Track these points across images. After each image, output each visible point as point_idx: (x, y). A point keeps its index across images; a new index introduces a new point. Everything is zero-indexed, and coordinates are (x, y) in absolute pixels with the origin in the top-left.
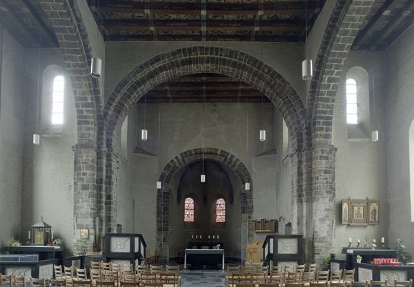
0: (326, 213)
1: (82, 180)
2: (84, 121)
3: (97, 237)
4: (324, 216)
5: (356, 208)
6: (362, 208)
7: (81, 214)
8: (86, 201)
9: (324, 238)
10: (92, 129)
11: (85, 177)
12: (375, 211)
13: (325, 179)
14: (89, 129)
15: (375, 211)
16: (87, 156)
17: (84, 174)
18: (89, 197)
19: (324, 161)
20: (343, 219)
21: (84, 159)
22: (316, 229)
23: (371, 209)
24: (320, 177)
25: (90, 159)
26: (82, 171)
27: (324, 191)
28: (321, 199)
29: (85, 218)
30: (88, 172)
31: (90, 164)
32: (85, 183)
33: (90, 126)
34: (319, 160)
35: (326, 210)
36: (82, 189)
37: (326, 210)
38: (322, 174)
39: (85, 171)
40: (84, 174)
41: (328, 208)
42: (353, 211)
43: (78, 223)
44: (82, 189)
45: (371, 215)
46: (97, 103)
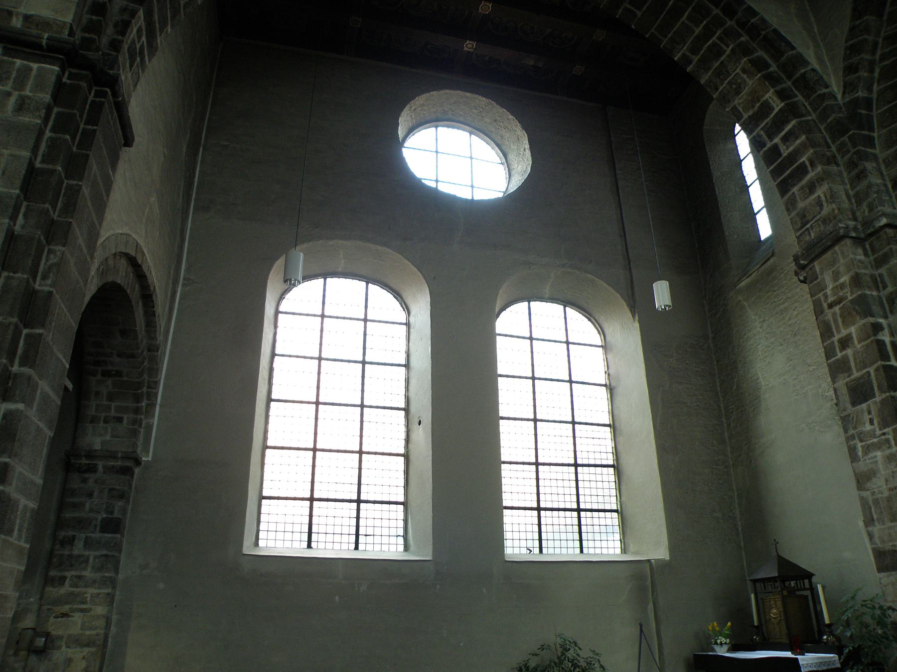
2: (790, 176)
8: (878, 446)
10: (820, 180)
11: (849, 352)
14: (811, 187)
16: (836, 276)
17: (845, 343)
18: (884, 424)
21: (829, 291)
25: (845, 279)
30: (853, 329)
31: (850, 298)
32: (856, 374)
33: (811, 175)
36: (854, 404)
39: (844, 333)
40: (845, 343)
44: (854, 404)
46: (807, 97)
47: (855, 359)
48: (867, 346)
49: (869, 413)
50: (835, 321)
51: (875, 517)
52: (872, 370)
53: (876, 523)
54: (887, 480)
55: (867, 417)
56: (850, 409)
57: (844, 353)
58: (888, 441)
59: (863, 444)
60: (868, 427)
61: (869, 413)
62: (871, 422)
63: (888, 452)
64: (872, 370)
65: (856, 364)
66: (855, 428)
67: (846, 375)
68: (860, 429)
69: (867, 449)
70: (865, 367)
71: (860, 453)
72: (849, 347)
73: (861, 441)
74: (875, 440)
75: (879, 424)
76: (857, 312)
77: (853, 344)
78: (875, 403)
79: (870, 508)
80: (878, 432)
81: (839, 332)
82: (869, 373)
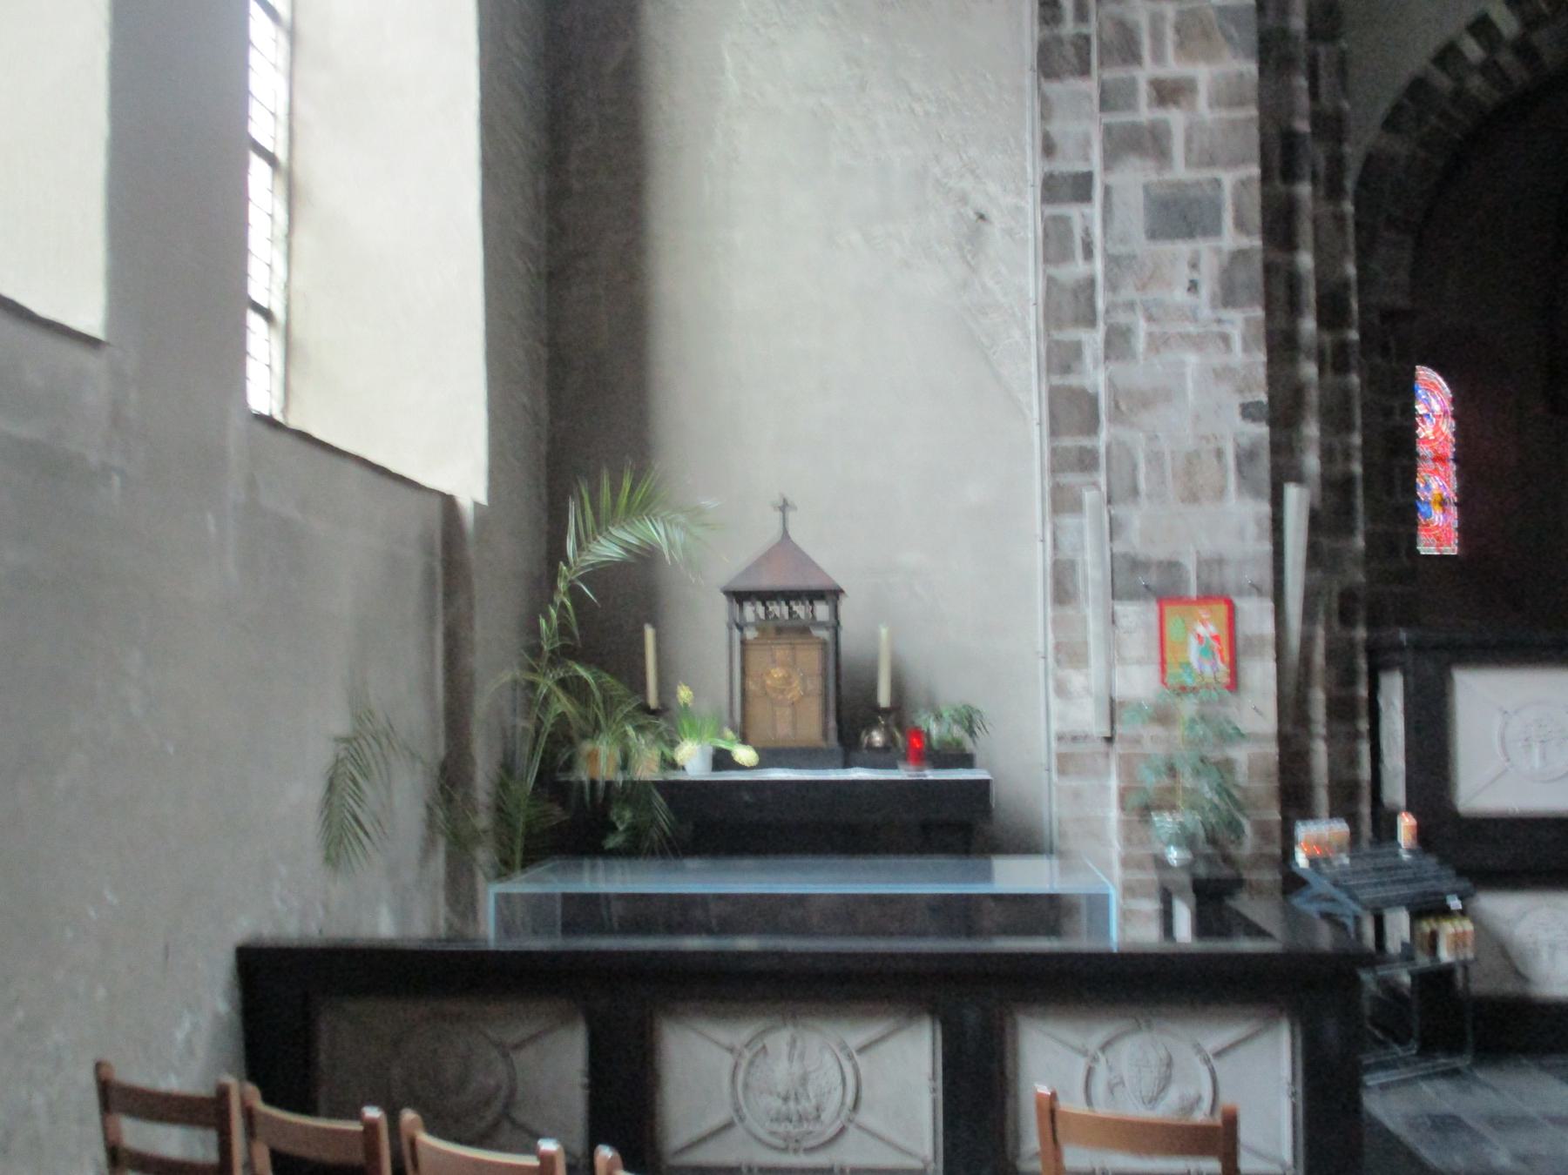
1: (1152, 143)
3: (1291, 677)
7: (1155, 459)
8: (1197, 342)
11: (1176, 118)
17: (1168, 93)
26: (1144, 73)
29: (1192, 497)
30: (1203, 74)
32: (1180, 171)
36: (1153, 234)
39: (1173, 68)
40: (1168, 93)
43: (1134, 541)
44: (1153, 234)
47: (1189, 140)
48: (1233, 124)
49: (1194, 266)
50: (1157, 37)
51: (1143, 485)
52: (1228, 179)
53: (1143, 499)
54: (1197, 417)
55: (1185, 274)
56: (1140, 244)
57: (1160, 114)
58: (1225, 339)
59: (1156, 329)
60: (1180, 295)
61: (1194, 266)
62: (1193, 287)
63: (1217, 359)
64: (1228, 179)
65: (1189, 149)
66: (1143, 287)
67: (1150, 164)
68: (1154, 293)
69: (1158, 343)
70: (1211, 162)
71: (1140, 343)
72: (1176, 103)
73: (1150, 318)
74: (1192, 329)
75: (1213, 298)
76: (1229, 39)
77: (1192, 106)
78: (1218, 251)
79: (1134, 467)
80: (1206, 312)
81: (1158, 57)
82: (1217, 183)
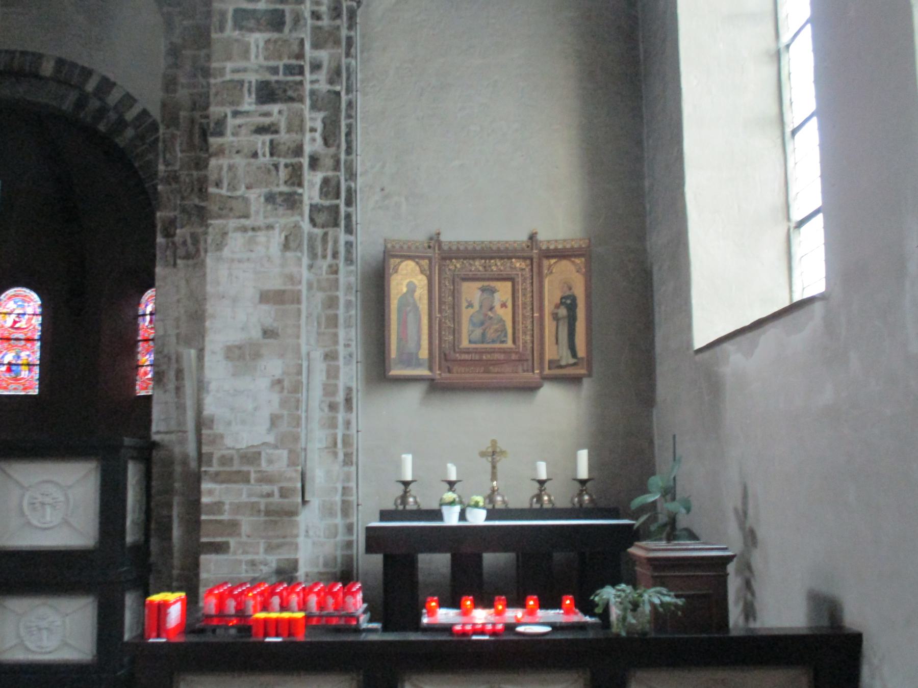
0: (266, 314)
4: (256, 334)
5: (471, 292)
6: (503, 291)
9: (251, 457)
12: (569, 303)
13: (261, 130)
15: (572, 307)
19: (257, 39)
20: (394, 353)
22: (211, 407)
23: (552, 294)
24: (231, 122)
27: (252, 195)
28: (236, 242)
34: (230, 32)
35: (265, 297)
37: (265, 297)
38: (248, 103)
41: (275, 284)
42: (455, 307)
45: (549, 325)
